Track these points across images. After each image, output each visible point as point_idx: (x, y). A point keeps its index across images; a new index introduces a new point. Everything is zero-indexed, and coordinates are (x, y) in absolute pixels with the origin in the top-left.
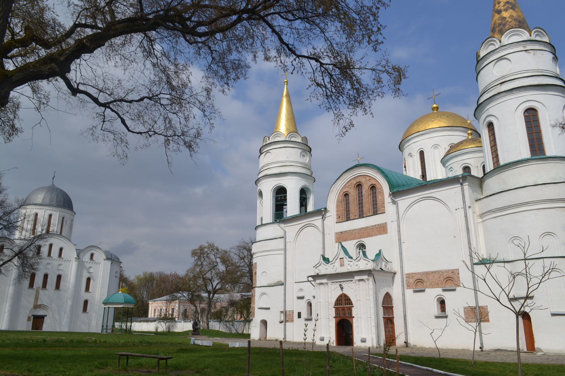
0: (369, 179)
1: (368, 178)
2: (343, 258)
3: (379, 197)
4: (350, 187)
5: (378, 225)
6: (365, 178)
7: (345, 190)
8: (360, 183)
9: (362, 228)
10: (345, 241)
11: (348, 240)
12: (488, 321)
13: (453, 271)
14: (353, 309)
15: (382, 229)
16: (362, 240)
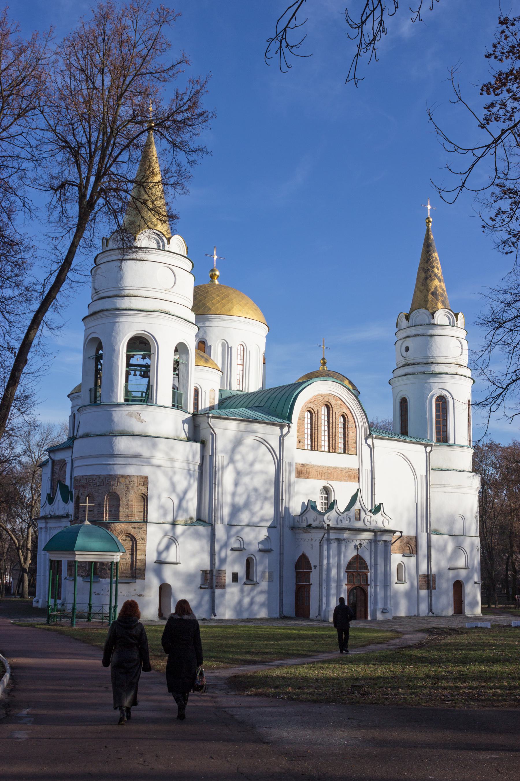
0: (341, 405)
1: (339, 402)
2: (360, 510)
3: (351, 434)
4: (316, 403)
5: (349, 469)
6: (336, 400)
7: (309, 406)
8: (329, 404)
9: (330, 467)
10: (308, 477)
11: (311, 478)
12: (434, 588)
13: (410, 538)
14: (369, 574)
15: (353, 475)
16: (330, 482)
